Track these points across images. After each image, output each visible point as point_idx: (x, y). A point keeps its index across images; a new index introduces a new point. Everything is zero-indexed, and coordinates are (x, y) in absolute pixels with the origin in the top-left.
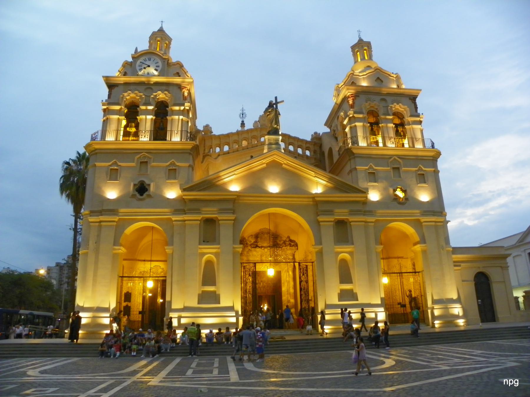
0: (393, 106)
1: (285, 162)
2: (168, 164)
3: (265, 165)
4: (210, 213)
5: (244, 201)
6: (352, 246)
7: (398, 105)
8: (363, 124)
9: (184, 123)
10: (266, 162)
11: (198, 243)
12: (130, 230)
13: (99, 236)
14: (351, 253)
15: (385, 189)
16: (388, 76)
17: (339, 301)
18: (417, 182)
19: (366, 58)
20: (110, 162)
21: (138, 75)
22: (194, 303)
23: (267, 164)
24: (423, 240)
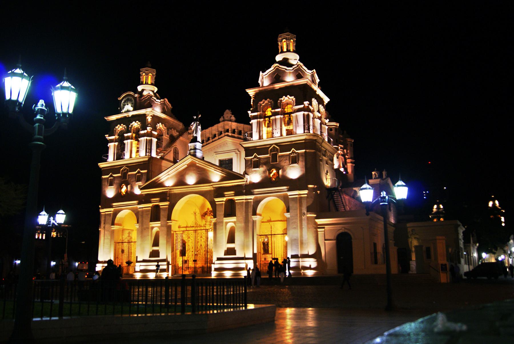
0: (282, 99)
1: (197, 162)
3: (186, 166)
4: (155, 202)
5: (174, 192)
6: (235, 217)
7: (286, 97)
8: (257, 121)
9: (148, 141)
10: (187, 163)
11: (149, 221)
12: (119, 215)
13: (105, 220)
14: (235, 222)
15: (264, 172)
16: (285, 71)
17: (225, 255)
18: (290, 163)
19: (285, 50)
20: (108, 175)
21: (122, 113)
22: (147, 258)
23: (187, 165)
24: (288, 211)
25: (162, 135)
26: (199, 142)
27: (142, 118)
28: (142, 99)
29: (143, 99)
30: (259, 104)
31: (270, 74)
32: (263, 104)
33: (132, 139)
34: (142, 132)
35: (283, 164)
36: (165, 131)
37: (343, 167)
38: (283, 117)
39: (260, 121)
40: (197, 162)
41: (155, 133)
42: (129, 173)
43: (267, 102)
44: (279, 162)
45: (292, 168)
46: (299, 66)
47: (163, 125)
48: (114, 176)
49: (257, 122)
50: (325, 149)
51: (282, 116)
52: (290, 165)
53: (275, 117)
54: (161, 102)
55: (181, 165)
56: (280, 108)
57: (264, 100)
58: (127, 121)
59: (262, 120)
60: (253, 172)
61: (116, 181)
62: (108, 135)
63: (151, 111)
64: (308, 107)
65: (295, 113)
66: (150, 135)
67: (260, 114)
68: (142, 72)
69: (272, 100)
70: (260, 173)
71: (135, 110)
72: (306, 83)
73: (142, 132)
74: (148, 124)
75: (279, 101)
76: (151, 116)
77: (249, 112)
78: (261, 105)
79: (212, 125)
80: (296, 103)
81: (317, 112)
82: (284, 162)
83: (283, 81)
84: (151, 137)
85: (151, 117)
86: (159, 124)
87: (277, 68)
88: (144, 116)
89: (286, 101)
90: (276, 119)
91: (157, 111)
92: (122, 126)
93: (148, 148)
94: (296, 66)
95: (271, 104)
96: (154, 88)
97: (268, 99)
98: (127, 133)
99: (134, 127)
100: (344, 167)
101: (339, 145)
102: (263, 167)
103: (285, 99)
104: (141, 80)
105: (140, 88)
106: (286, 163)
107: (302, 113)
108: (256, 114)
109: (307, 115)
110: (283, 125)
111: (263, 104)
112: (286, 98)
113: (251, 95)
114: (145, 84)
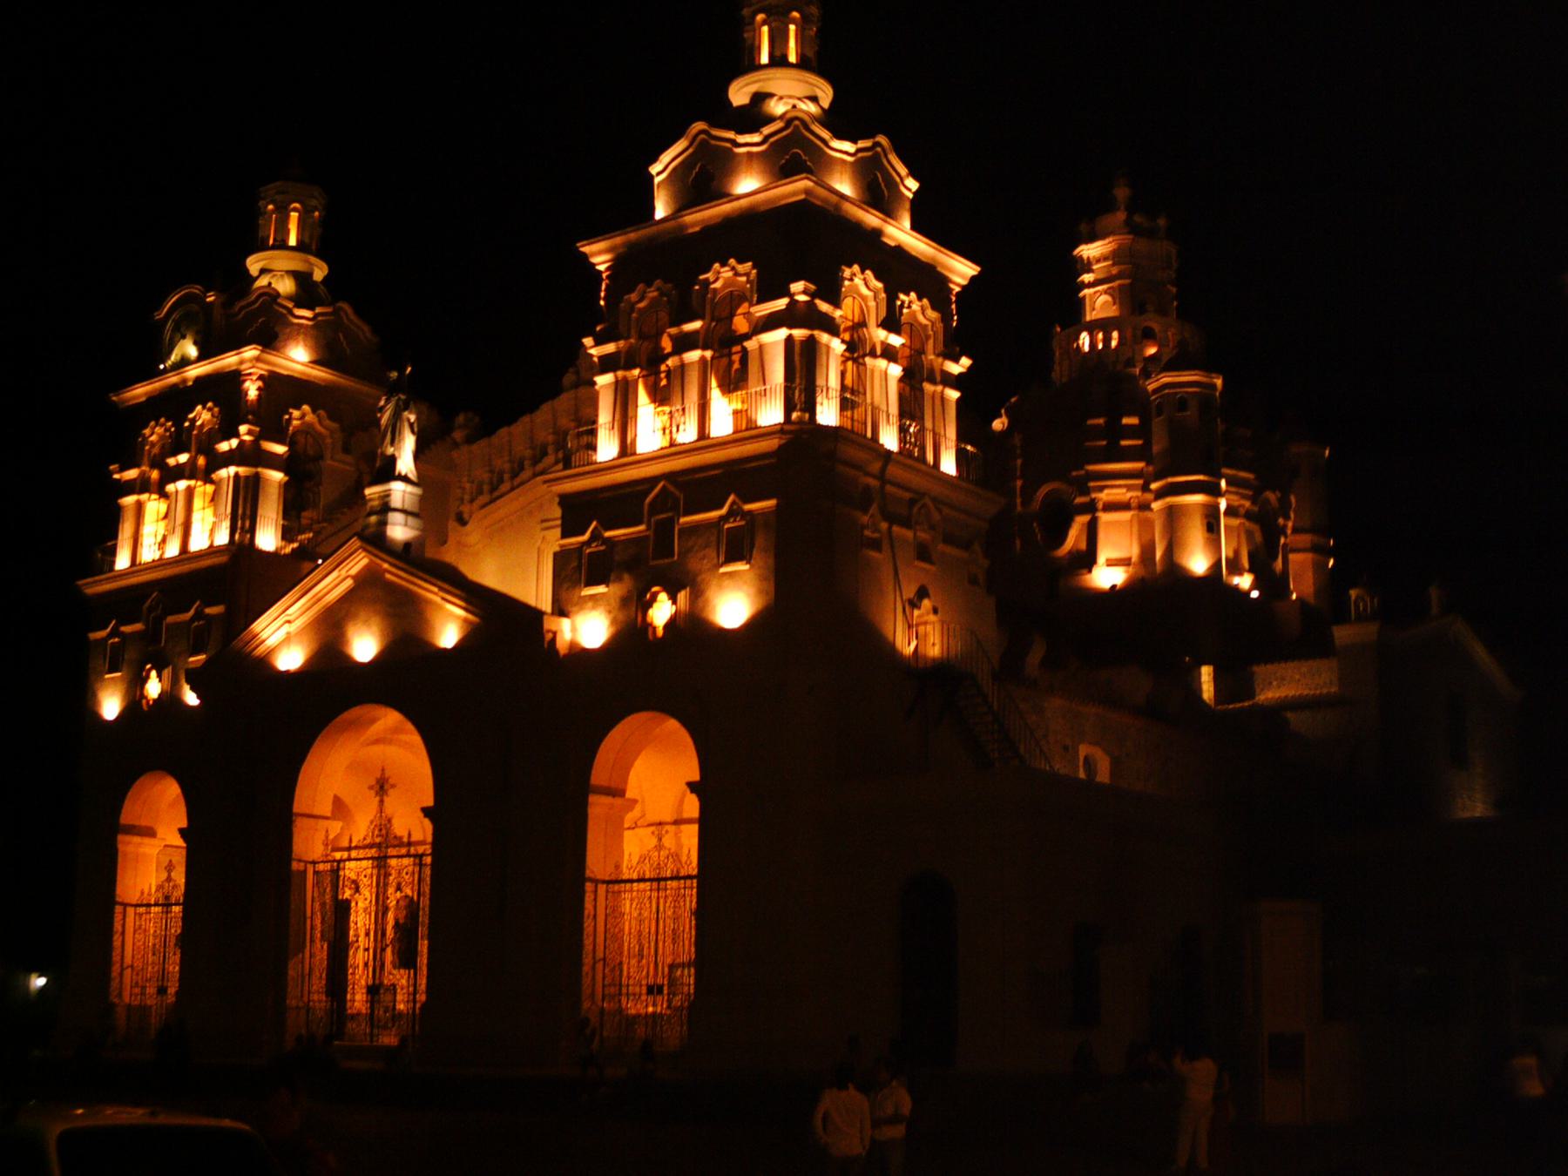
0: (710, 275)
2: (192, 612)
3: (349, 583)
7: (727, 269)
8: (616, 377)
10: (353, 572)
15: (625, 602)
21: (165, 371)
23: (354, 577)
25: (321, 457)
26: (405, 479)
27: (224, 388)
28: (237, 309)
29: (240, 310)
30: (622, 305)
31: (675, 169)
32: (641, 305)
33: (190, 478)
34: (224, 446)
35: (693, 564)
36: (332, 437)
37: (1250, 571)
38: (713, 358)
39: (625, 379)
40: (386, 566)
41: (280, 449)
42: (170, 619)
43: (655, 294)
44: (679, 555)
45: (727, 582)
46: (797, 122)
47: (321, 412)
48: (123, 633)
49: (617, 382)
50: (908, 489)
51: (708, 354)
52: (722, 570)
53: (682, 360)
54: (320, 318)
55: (333, 583)
56: (701, 317)
57: (641, 286)
58: (177, 402)
59: (636, 372)
60: (585, 602)
61: (130, 654)
62: (119, 467)
63: (258, 359)
64: (810, 305)
65: (754, 338)
66: (250, 455)
67: (631, 347)
68: (263, 199)
69: (670, 285)
70: (609, 605)
71: (203, 356)
72: (802, 197)
73: (224, 446)
74: (247, 414)
75: (697, 287)
76: (261, 378)
77: (588, 341)
78: (633, 305)
79: (532, 408)
80: (759, 291)
81: (878, 326)
82: (702, 554)
83: (725, 195)
84: (256, 466)
85: (260, 383)
86: (298, 408)
87: (703, 140)
88: (234, 378)
89: (725, 286)
90: (686, 368)
91: (298, 357)
92: (162, 425)
93: (240, 512)
94: (778, 125)
95: (669, 301)
96: (307, 261)
97: (658, 283)
98: (175, 453)
99: (202, 425)
100: (1259, 569)
101: (1225, 471)
102: (619, 579)
103: (723, 276)
104: (260, 234)
105: (254, 264)
106: (705, 561)
107: (781, 334)
108: (610, 348)
109: (802, 342)
110: (715, 393)
111: (641, 305)
112: (726, 273)
113: (602, 268)
114: (274, 248)
